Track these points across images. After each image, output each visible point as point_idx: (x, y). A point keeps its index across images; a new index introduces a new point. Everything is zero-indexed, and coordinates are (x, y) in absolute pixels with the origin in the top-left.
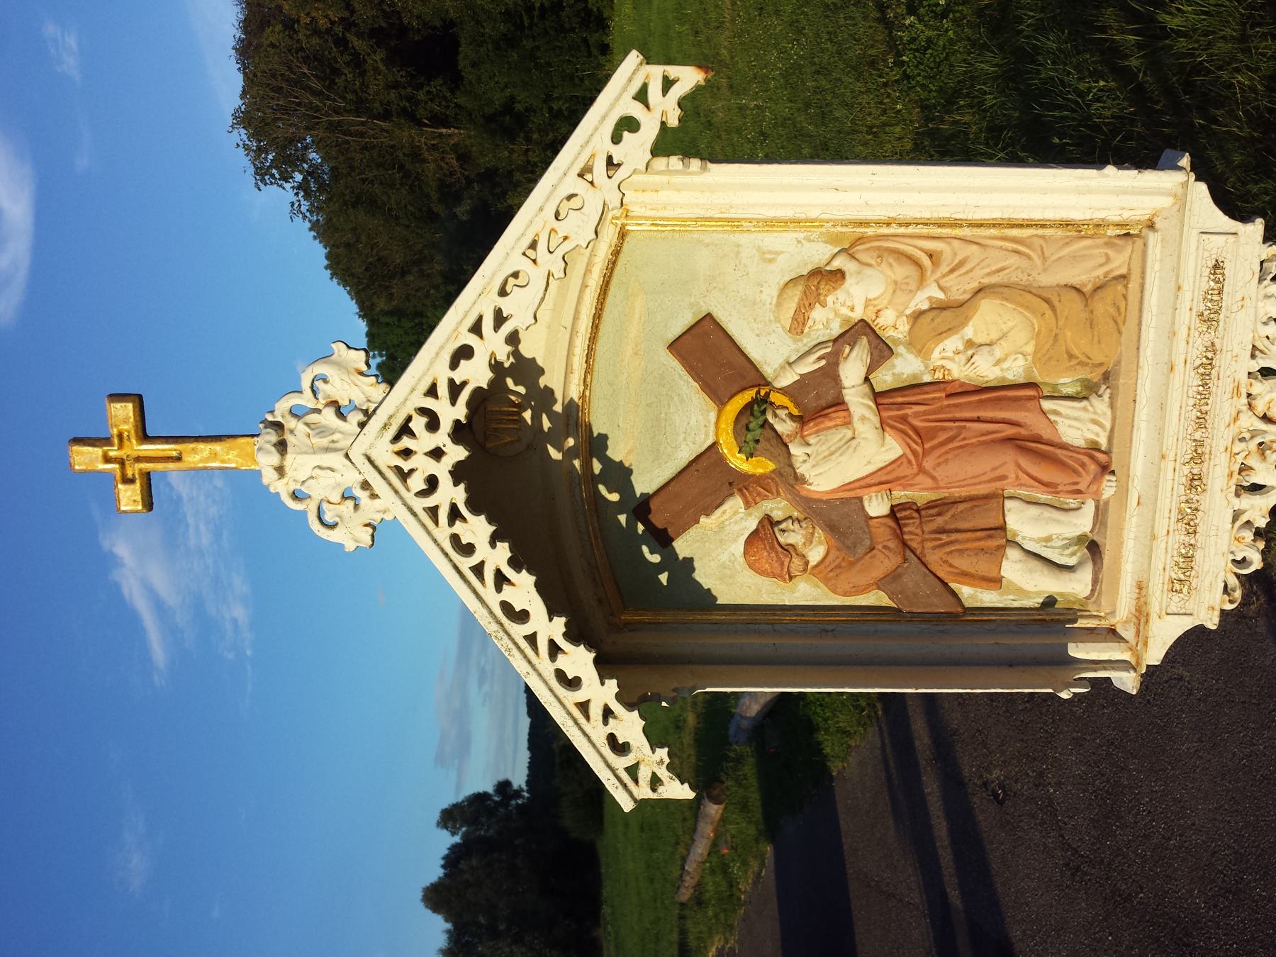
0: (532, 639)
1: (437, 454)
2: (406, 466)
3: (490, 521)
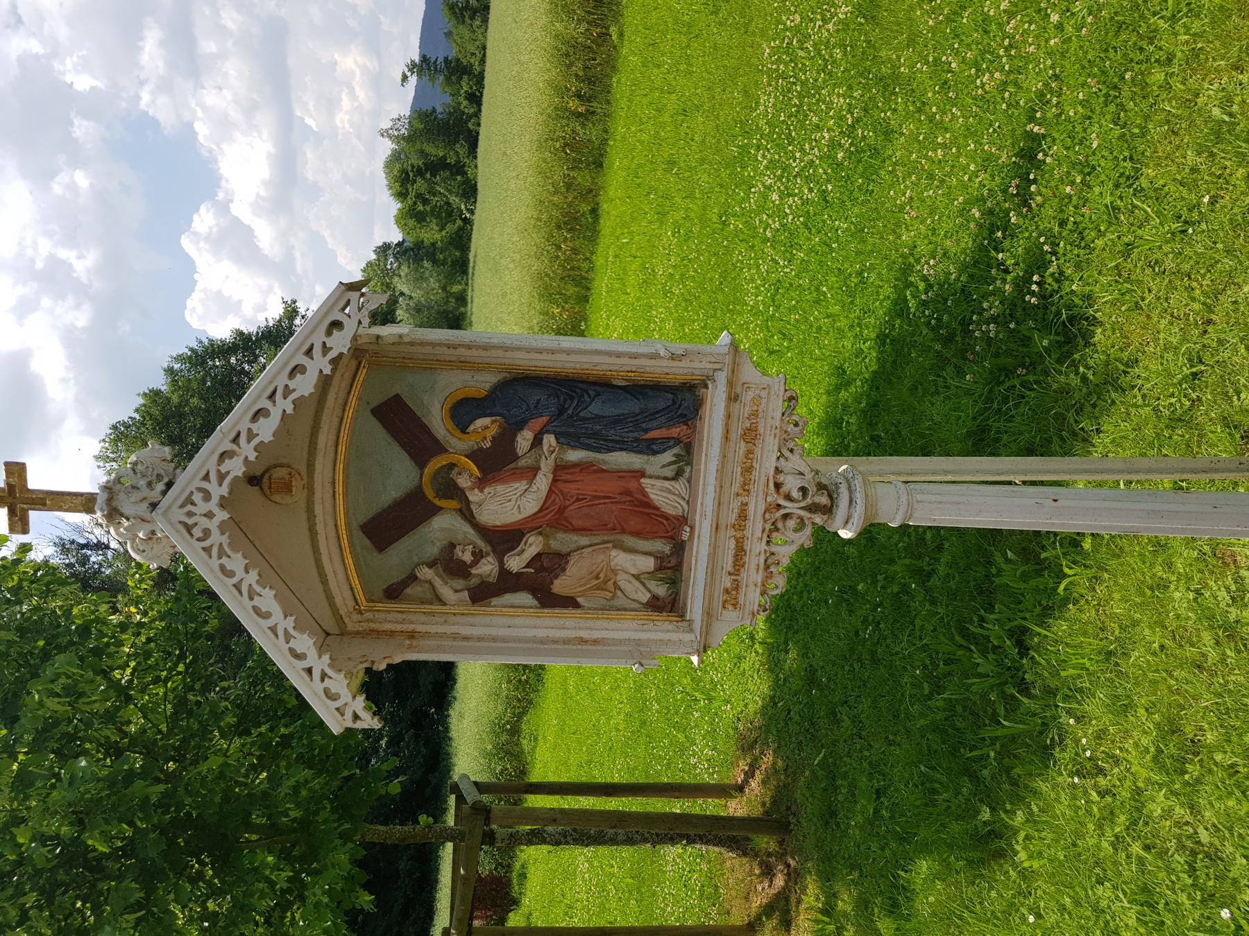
0: (273, 629)
1: (209, 515)
2: (190, 521)
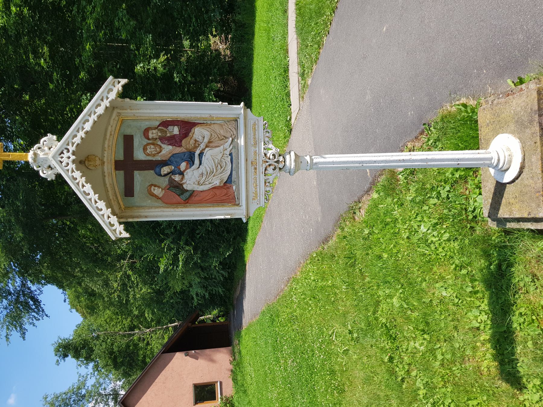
0: (90, 199)
2: (62, 160)
3: (81, 172)
